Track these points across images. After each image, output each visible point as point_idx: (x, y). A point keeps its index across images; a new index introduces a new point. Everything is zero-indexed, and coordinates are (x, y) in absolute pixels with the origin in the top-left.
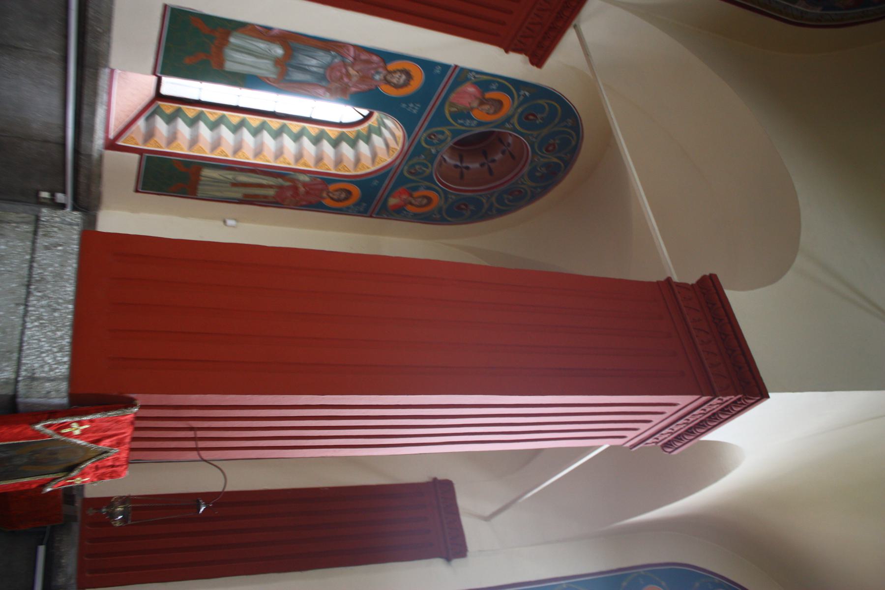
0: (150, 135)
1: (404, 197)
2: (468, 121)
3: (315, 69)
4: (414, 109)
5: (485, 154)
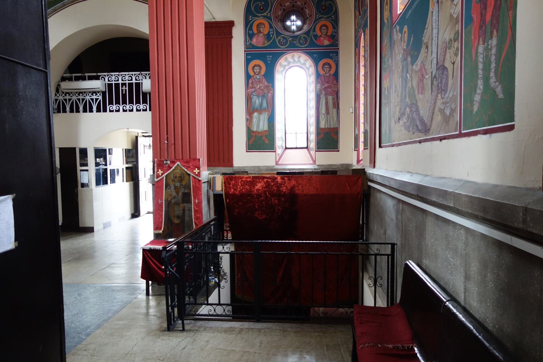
2: (271, 33)
3: (260, 100)
4: (269, 58)
5: (303, 8)
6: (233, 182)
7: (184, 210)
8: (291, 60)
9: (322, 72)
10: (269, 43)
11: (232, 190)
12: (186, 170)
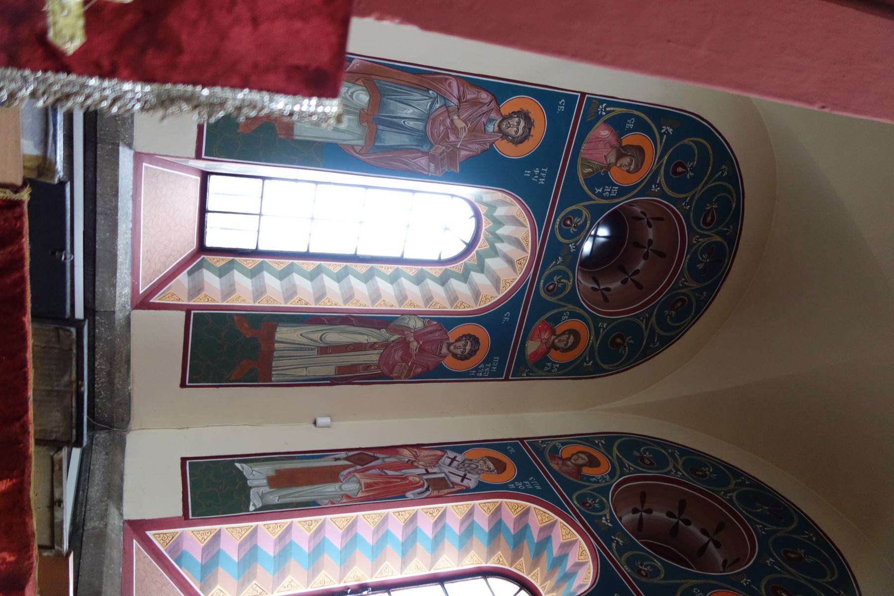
0: (197, 289)
1: (545, 336)
3: (411, 124)
4: (539, 176)
10: (582, 181)
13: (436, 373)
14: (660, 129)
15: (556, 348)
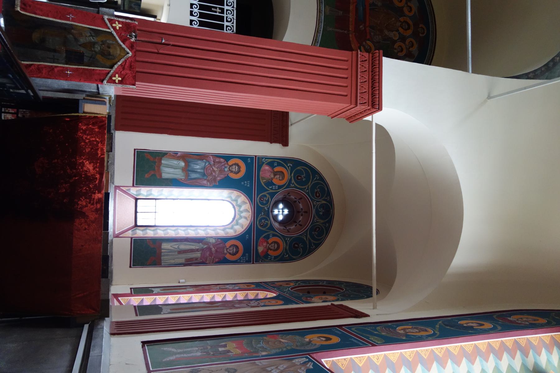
1: (265, 244)
2: (274, 187)
3: (199, 170)
4: (247, 184)
5: (295, 222)
6: (97, 130)
7: (55, 51)
8: (242, 209)
9: (228, 244)
10: (263, 185)
11: (84, 128)
12: (119, 63)
13: (224, 261)
14: (287, 165)
15: (271, 250)
